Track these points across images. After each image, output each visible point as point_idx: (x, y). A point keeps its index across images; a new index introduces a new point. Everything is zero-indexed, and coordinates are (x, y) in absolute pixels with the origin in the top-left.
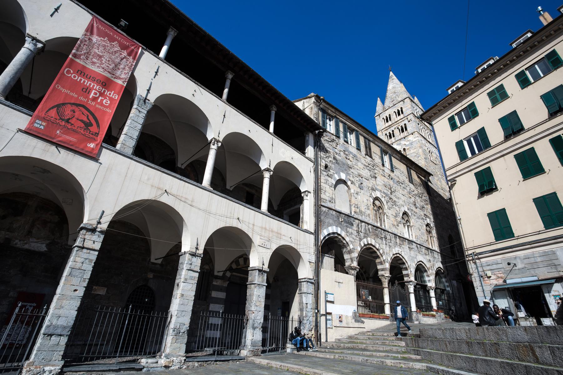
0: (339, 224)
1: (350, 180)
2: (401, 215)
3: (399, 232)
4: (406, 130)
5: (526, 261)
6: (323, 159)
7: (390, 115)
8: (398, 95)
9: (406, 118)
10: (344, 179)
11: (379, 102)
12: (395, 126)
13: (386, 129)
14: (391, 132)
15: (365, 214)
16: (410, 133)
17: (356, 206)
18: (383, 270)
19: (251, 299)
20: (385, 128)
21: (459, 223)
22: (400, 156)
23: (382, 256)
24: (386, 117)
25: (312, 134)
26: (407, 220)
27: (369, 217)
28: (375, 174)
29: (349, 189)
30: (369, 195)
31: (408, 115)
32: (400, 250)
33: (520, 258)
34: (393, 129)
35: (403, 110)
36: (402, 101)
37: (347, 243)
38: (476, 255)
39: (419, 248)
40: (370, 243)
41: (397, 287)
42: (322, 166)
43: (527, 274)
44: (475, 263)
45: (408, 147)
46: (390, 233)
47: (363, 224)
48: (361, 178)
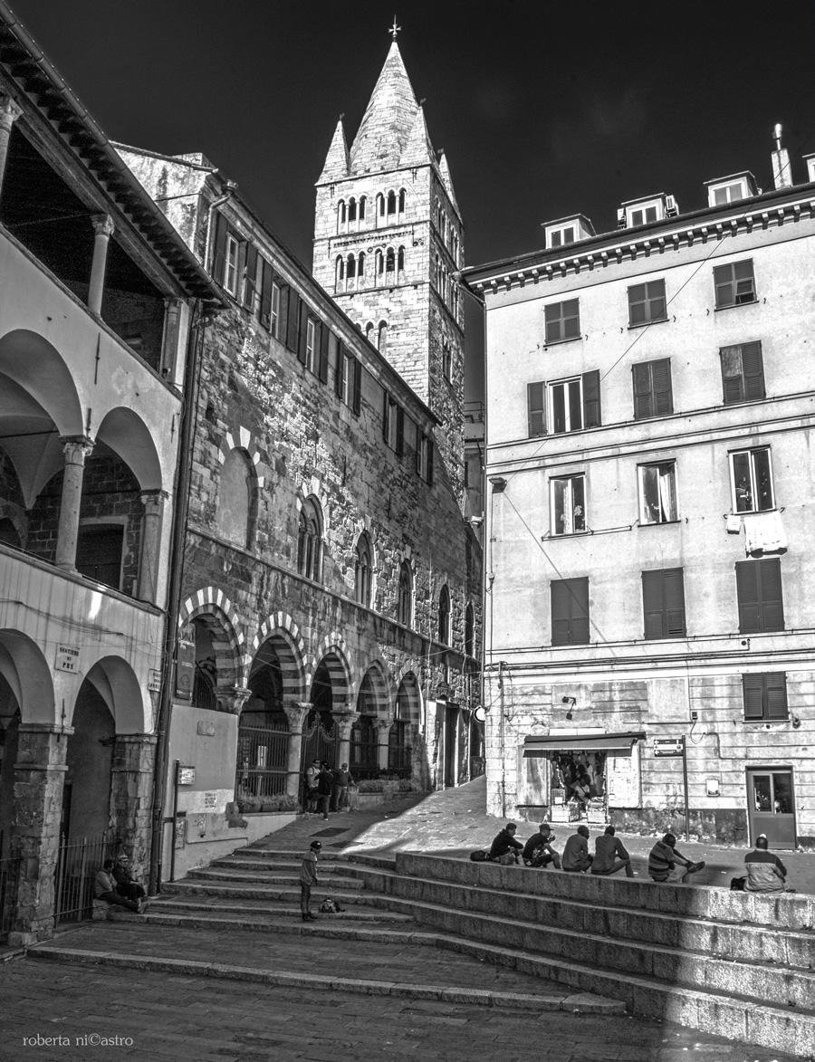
0: (219, 581)
1: (259, 449)
2: (355, 541)
3: (344, 590)
4: (401, 267)
5: (595, 696)
6: (205, 386)
8: (403, 141)
9: (409, 229)
11: (338, 138)
12: (371, 243)
13: (343, 240)
14: (356, 257)
15: (281, 548)
16: (411, 280)
17: (264, 527)
18: (295, 690)
19: (31, 809)
21: (488, 586)
22: (380, 368)
23: (301, 657)
24: (352, 200)
26: (365, 553)
27: (288, 555)
29: (252, 474)
30: (295, 491)
31: (417, 223)
32: (340, 637)
33: (586, 688)
35: (407, 200)
36: (409, 169)
37: (232, 630)
38: (505, 669)
39: (378, 627)
41: (318, 727)
42: (200, 410)
43: (589, 721)
44: (501, 686)
46: (327, 593)
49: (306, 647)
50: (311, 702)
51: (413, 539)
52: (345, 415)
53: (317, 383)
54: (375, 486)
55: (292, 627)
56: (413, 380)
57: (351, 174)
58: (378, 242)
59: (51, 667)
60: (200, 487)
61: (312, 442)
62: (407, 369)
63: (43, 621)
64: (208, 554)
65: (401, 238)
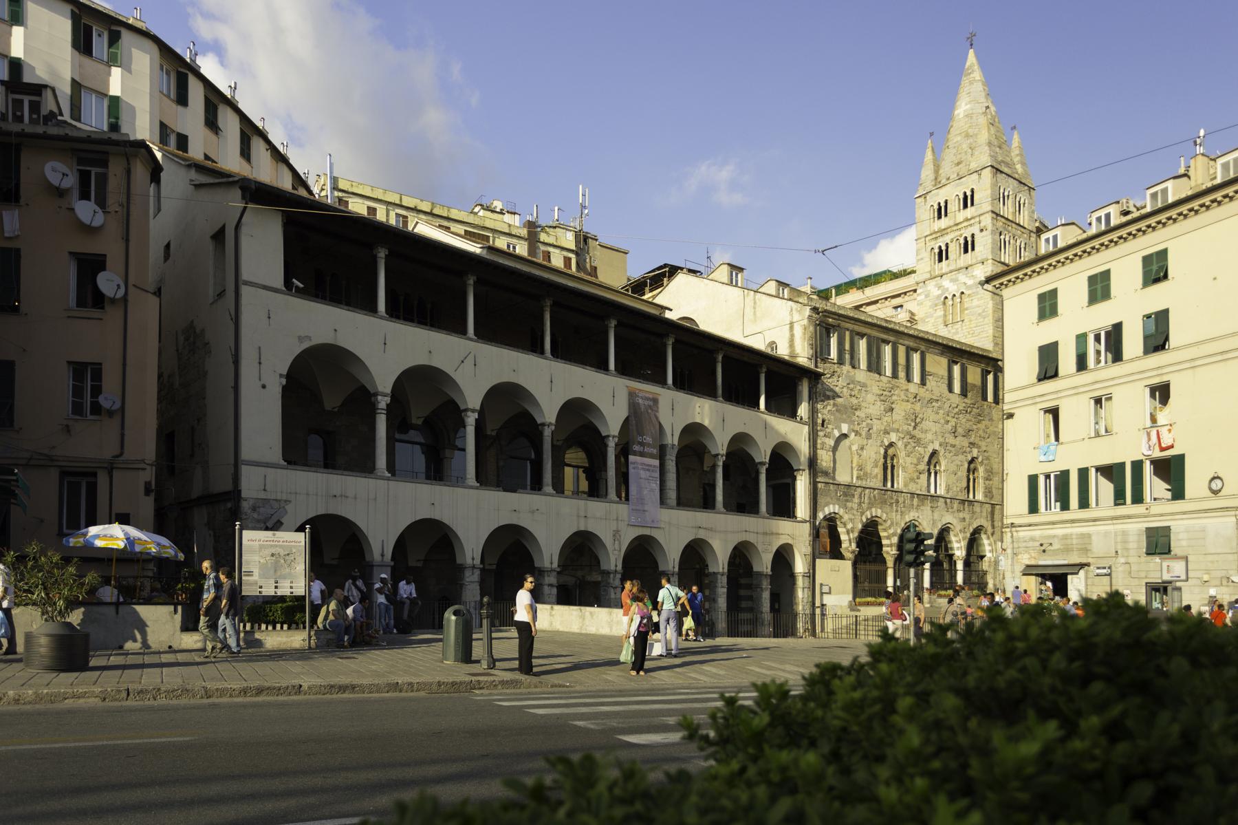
1: (853, 431)
2: (926, 459)
3: (919, 487)
4: (973, 249)
7: (946, 202)
10: (846, 433)
11: (929, 156)
13: (934, 236)
14: (944, 248)
16: (979, 259)
20: (931, 234)
25: (806, 377)
28: (892, 403)
32: (917, 514)
34: (949, 242)
40: (874, 515)
45: (970, 292)
47: (868, 490)
48: (869, 421)
49: (892, 523)
50: (898, 551)
51: (980, 443)
52: (913, 388)
53: (890, 379)
54: (942, 421)
55: (882, 515)
56: (982, 332)
57: (938, 184)
58: (958, 233)
59: (760, 551)
60: (822, 460)
61: (890, 414)
62: (979, 324)
63: (756, 535)
64: (829, 490)
65: (972, 228)
